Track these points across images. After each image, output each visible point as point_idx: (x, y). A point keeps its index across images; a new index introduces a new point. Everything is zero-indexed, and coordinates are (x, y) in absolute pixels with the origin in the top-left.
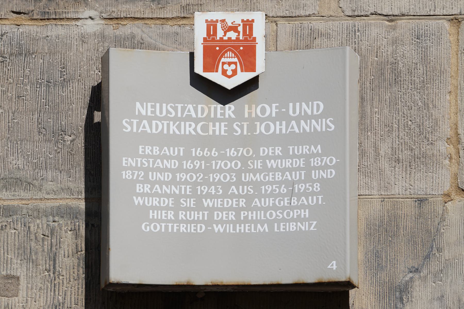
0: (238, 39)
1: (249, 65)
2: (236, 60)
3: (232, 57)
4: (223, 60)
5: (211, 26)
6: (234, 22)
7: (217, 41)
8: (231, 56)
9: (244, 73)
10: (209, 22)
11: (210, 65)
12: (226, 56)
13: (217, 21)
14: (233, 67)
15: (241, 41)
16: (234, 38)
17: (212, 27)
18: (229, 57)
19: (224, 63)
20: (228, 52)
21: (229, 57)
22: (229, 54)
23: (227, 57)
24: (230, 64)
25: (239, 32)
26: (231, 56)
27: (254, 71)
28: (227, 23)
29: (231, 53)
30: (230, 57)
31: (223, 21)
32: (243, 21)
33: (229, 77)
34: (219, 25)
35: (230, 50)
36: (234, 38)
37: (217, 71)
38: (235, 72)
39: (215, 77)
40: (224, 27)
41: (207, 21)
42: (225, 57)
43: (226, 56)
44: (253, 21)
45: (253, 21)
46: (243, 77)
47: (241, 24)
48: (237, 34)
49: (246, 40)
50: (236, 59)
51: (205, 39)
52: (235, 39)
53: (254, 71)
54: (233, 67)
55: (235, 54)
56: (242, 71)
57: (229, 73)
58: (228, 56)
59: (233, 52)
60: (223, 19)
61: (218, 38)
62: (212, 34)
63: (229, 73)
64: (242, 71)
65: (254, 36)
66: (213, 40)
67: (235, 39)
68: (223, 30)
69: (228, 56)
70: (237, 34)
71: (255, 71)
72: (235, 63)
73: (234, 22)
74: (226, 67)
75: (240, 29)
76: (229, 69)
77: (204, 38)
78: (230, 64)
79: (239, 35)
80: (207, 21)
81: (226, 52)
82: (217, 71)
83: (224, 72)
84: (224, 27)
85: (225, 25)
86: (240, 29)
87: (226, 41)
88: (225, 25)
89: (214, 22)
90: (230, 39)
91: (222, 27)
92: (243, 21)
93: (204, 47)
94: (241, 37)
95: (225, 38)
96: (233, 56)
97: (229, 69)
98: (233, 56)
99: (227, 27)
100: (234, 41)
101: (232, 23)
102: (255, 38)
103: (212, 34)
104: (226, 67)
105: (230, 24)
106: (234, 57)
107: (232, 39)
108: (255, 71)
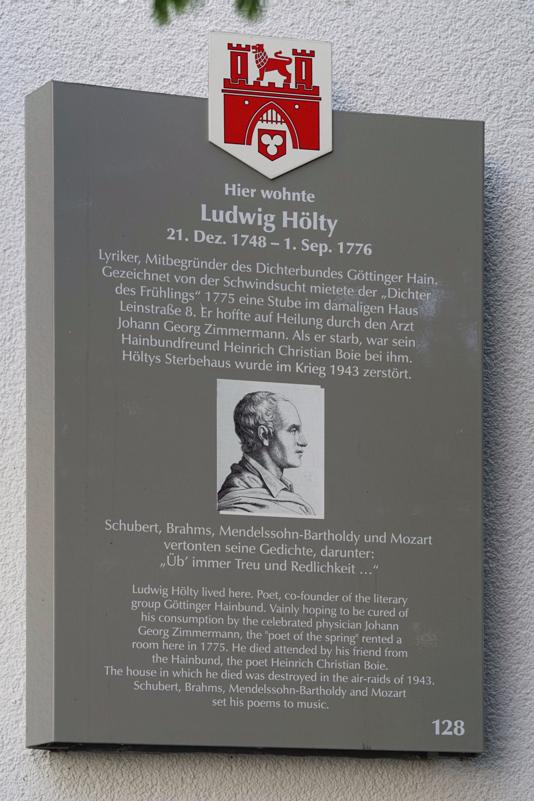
2: (284, 127)
3: (277, 122)
4: (260, 125)
6: (280, 52)
7: (250, 87)
8: (274, 119)
9: (299, 150)
11: (236, 132)
12: (265, 118)
13: (248, 48)
14: (278, 140)
15: (293, 91)
16: (279, 84)
17: (239, 57)
18: (271, 121)
19: (262, 132)
21: (271, 121)
22: (271, 114)
23: (267, 121)
24: (272, 133)
25: (288, 75)
26: (274, 119)
28: (265, 54)
29: (274, 112)
30: (272, 121)
31: (260, 48)
32: (295, 52)
33: (272, 158)
35: (272, 107)
36: (279, 84)
37: (249, 143)
38: (282, 150)
39: (246, 153)
41: (230, 46)
42: (262, 121)
43: (265, 118)
44: (312, 53)
45: (312, 53)
46: (296, 157)
47: (293, 58)
48: (285, 78)
49: (300, 90)
50: (284, 124)
52: (281, 86)
54: (278, 140)
55: (283, 116)
56: (295, 147)
57: (272, 151)
58: (270, 119)
59: (278, 112)
60: (261, 43)
61: (251, 83)
62: (239, 72)
63: (272, 151)
64: (295, 147)
65: (314, 84)
66: (244, 85)
67: (281, 86)
68: (259, 66)
69: (270, 119)
70: (285, 78)
71: (318, 149)
72: (282, 134)
73: (280, 52)
74: (266, 139)
75: (291, 68)
76: (272, 144)
77: (225, 80)
78: (272, 133)
79: (288, 80)
80: (230, 46)
81: (265, 110)
82: (249, 143)
83: (263, 149)
85: (263, 58)
86: (291, 68)
87: (264, 89)
88: (263, 58)
90: (271, 85)
91: (257, 62)
92: (295, 52)
94: (292, 85)
95: (264, 83)
96: (279, 119)
97: (272, 144)
98: (279, 119)
99: (265, 61)
101: (276, 55)
102: (317, 89)
103: (239, 72)
104: (266, 139)
105: (271, 56)
106: (281, 122)
107: (277, 86)
108: (318, 149)
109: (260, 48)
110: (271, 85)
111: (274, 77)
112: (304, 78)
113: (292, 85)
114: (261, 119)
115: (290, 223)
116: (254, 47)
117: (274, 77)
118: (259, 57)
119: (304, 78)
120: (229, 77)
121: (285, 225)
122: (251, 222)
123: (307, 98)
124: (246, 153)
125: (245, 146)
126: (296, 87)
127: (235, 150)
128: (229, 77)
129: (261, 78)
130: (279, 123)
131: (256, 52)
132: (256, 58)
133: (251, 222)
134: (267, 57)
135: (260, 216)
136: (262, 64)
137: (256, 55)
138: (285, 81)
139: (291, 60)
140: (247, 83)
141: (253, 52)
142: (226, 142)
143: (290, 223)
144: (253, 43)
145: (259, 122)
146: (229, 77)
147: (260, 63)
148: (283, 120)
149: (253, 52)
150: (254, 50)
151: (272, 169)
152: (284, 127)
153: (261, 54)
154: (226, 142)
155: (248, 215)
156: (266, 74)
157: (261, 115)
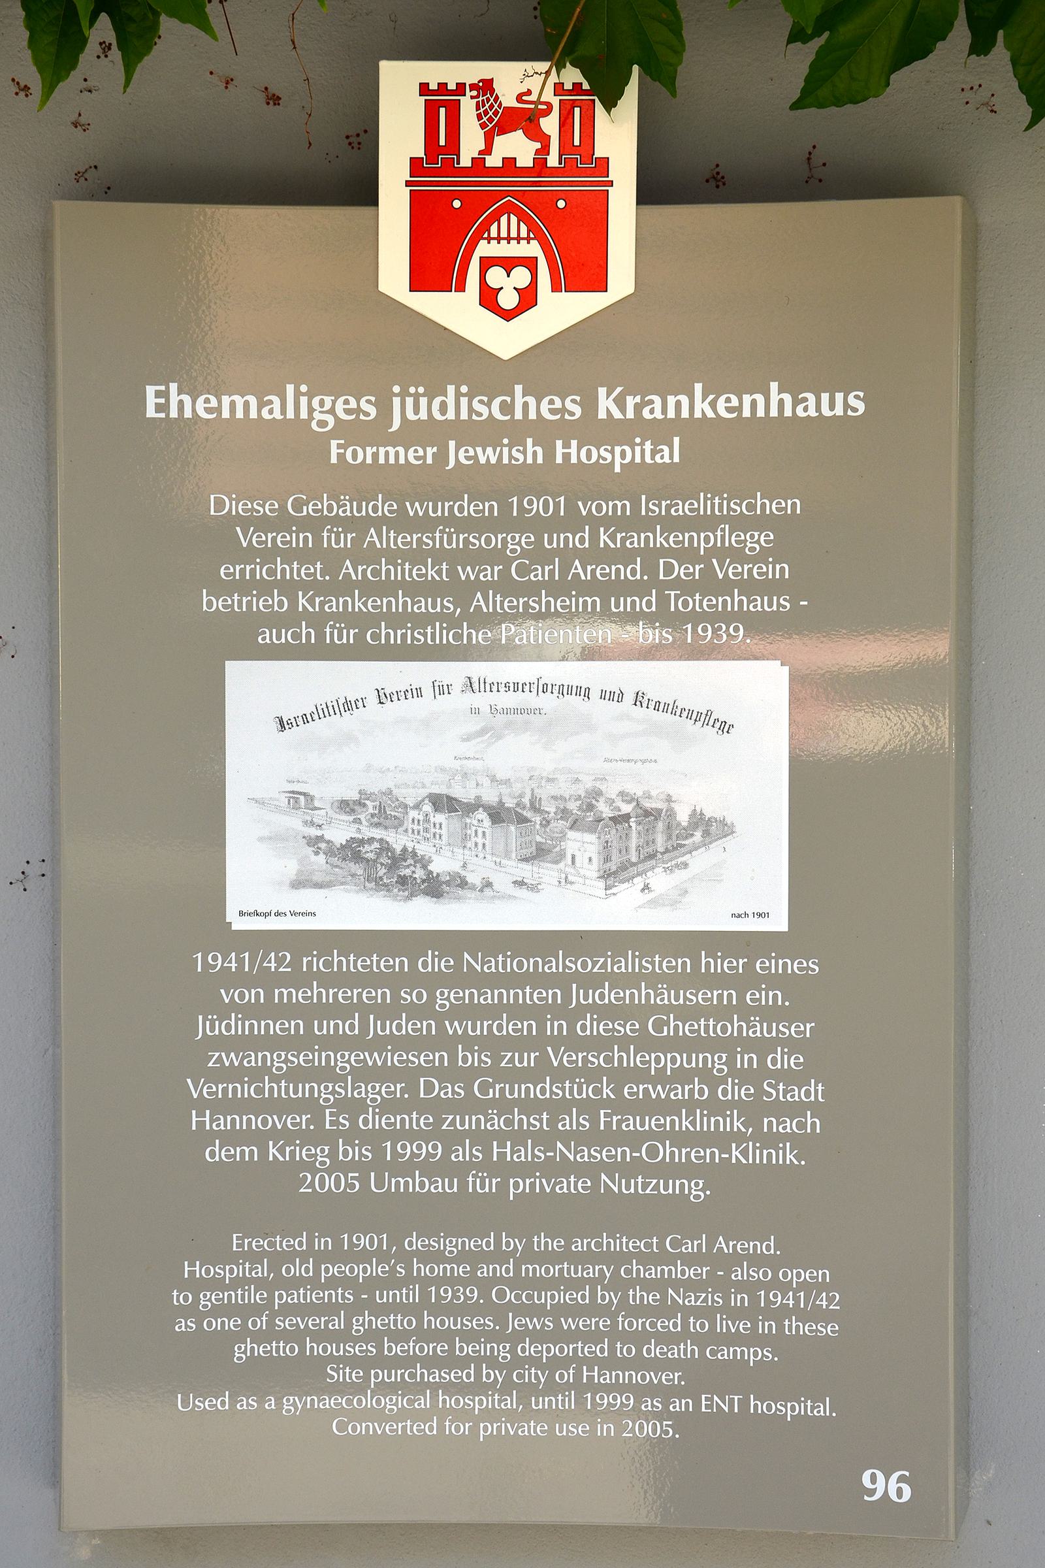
0: (540, 164)
1: (583, 269)
2: (533, 249)
3: (518, 239)
4: (484, 249)
5: (440, 104)
7: (465, 171)
8: (514, 234)
9: (563, 296)
10: (433, 93)
11: (434, 267)
13: (461, 89)
14: (521, 276)
15: (554, 171)
16: (525, 160)
17: (442, 111)
18: (510, 238)
19: (487, 263)
20: (504, 219)
21: (510, 238)
22: (508, 224)
24: (508, 264)
25: (545, 140)
26: (514, 234)
27: (600, 285)
28: (497, 98)
29: (514, 219)
31: (486, 86)
33: (509, 315)
34: (468, 106)
35: (509, 209)
36: (525, 160)
37: (461, 288)
38: (528, 298)
40: (486, 113)
41: (424, 89)
42: (489, 239)
43: (494, 233)
47: (555, 101)
48: (538, 145)
49: (567, 168)
50: (534, 243)
51: (415, 163)
53: (600, 285)
54: (521, 276)
56: (556, 288)
57: (508, 300)
58: (504, 234)
61: (466, 162)
62: (442, 142)
63: (508, 300)
64: (556, 288)
66: (451, 168)
68: (483, 126)
69: (504, 234)
70: (538, 145)
72: (530, 263)
74: (496, 276)
75: (550, 125)
76: (508, 286)
78: (508, 264)
79: (545, 149)
80: (424, 89)
82: (461, 288)
83: (488, 298)
84: (486, 113)
85: (491, 107)
86: (550, 125)
87: (494, 171)
88: (491, 107)
89: (452, 93)
90: (509, 162)
91: (479, 117)
93: (416, 200)
94: (553, 160)
95: (494, 161)
97: (508, 286)
98: (524, 234)
100: (525, 171)
101: (519, 98)
103: (442, 142)
104: (496, 276)
105: (509, 101)
106: (528, 239)
109: (486, 86)
110: (509, 162)
111: (516, 147)
112: (577, 142)
113: (553, 160)
114: (486, 235)
115: (567, 457)
116: (473, 87)
117: (516, 147)
118: (484, 105)
119: (577, 142)
120: (422, 155)
121: (559, 460)
122: (493, 461)
123: (581, 184)
124: (455, 311)
125: (453, 294)
126: (560, 163)
127: (431, 304)
128: (422, 155)
129: (488, 150)
130: (523, 242)
131: (477, 97)
132: (478, 108)
133: (493, 461)
134: (500, 105)
135: (506, 450)
136: (491, 120)
137: (478, 103)
138: (537, 152)
139: (549, 105)
140: (458, 163)
141: (472, 97)
142: (414, 287)
143: (567, 457)
144: (470, 80)
145: (483, 243)
146: (420, 153)
147: (485, 119)
148: (532, 235)
149: (472, 97)
150: (474, 93)
151: (505, 340)
152: (533, 249)
153: (488, 100)
154: (414, 287)
155: (489, 450)
156: (498, 140)
157: (486, 226)
